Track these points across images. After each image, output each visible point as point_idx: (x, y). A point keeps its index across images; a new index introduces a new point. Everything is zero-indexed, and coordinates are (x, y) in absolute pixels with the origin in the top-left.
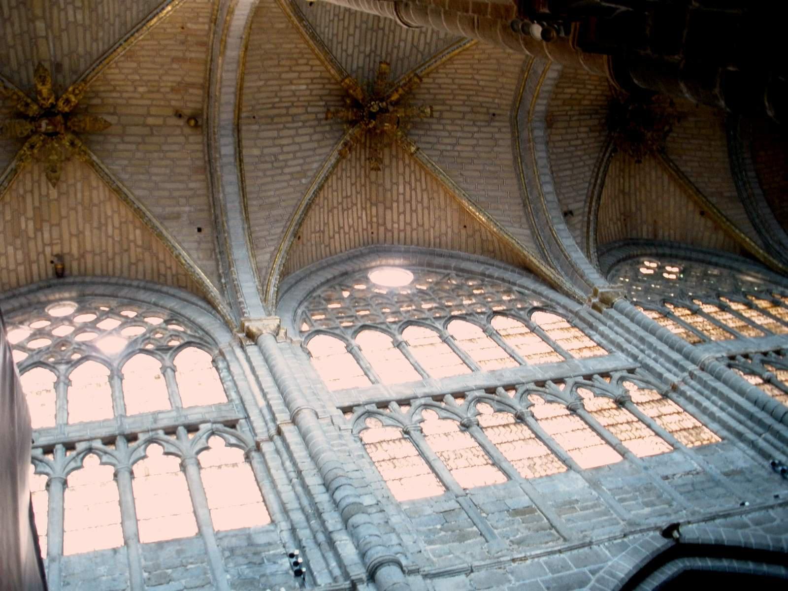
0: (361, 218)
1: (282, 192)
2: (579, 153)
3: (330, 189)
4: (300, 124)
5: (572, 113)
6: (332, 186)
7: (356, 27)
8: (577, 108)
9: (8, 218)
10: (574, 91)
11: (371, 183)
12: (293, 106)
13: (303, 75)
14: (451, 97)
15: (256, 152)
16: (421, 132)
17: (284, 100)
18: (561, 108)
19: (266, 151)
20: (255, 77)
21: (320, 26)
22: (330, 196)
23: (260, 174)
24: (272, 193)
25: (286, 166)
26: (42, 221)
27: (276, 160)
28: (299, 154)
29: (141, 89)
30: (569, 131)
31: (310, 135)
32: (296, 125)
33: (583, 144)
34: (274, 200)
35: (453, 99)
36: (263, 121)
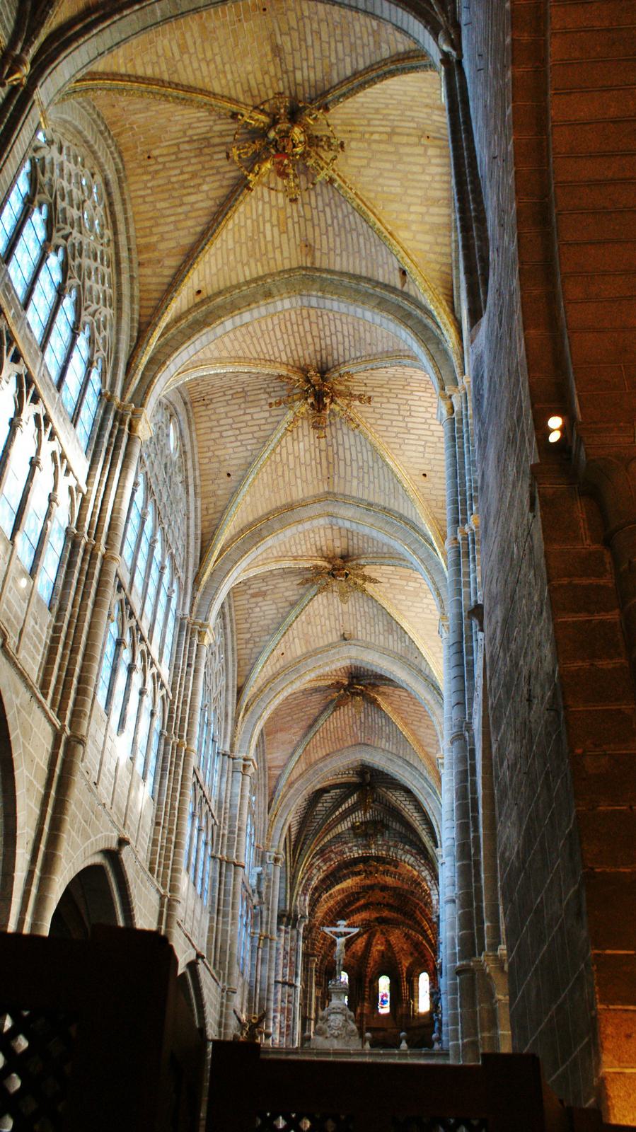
0: (420, 397)
1: (386, 476)
2: (340, 216)
3: (390, 429)
4: (334, 440)
5: (295, 215)
6: (387, 426)
7: (245, 414)
8: (289, 210)
9: (404, 598)
10: (268, 226)
11: (388, 384)
12: (319, 447)
13: (290, 451)
14: (296, 335)
15: (355, 482)
16: (335, 352)
17: (313, 457)
18: (291, 235)
19: (355, 474)
20: (294, 489)
21: (246, 457)
22: (396, 429)
23: (372, 486)
24: (387, 484)
25: (368, 462)
26: (410, 576)
27: (362, 468)
28: (359, 449)
29: (312, 535)
30: (316, 222)
31: (343, 434)
32: (335, 444)
33: (329, 205)
34: (392, 486)
35: (299, 332)
36: (331, 471)
